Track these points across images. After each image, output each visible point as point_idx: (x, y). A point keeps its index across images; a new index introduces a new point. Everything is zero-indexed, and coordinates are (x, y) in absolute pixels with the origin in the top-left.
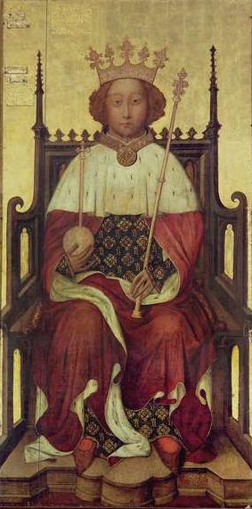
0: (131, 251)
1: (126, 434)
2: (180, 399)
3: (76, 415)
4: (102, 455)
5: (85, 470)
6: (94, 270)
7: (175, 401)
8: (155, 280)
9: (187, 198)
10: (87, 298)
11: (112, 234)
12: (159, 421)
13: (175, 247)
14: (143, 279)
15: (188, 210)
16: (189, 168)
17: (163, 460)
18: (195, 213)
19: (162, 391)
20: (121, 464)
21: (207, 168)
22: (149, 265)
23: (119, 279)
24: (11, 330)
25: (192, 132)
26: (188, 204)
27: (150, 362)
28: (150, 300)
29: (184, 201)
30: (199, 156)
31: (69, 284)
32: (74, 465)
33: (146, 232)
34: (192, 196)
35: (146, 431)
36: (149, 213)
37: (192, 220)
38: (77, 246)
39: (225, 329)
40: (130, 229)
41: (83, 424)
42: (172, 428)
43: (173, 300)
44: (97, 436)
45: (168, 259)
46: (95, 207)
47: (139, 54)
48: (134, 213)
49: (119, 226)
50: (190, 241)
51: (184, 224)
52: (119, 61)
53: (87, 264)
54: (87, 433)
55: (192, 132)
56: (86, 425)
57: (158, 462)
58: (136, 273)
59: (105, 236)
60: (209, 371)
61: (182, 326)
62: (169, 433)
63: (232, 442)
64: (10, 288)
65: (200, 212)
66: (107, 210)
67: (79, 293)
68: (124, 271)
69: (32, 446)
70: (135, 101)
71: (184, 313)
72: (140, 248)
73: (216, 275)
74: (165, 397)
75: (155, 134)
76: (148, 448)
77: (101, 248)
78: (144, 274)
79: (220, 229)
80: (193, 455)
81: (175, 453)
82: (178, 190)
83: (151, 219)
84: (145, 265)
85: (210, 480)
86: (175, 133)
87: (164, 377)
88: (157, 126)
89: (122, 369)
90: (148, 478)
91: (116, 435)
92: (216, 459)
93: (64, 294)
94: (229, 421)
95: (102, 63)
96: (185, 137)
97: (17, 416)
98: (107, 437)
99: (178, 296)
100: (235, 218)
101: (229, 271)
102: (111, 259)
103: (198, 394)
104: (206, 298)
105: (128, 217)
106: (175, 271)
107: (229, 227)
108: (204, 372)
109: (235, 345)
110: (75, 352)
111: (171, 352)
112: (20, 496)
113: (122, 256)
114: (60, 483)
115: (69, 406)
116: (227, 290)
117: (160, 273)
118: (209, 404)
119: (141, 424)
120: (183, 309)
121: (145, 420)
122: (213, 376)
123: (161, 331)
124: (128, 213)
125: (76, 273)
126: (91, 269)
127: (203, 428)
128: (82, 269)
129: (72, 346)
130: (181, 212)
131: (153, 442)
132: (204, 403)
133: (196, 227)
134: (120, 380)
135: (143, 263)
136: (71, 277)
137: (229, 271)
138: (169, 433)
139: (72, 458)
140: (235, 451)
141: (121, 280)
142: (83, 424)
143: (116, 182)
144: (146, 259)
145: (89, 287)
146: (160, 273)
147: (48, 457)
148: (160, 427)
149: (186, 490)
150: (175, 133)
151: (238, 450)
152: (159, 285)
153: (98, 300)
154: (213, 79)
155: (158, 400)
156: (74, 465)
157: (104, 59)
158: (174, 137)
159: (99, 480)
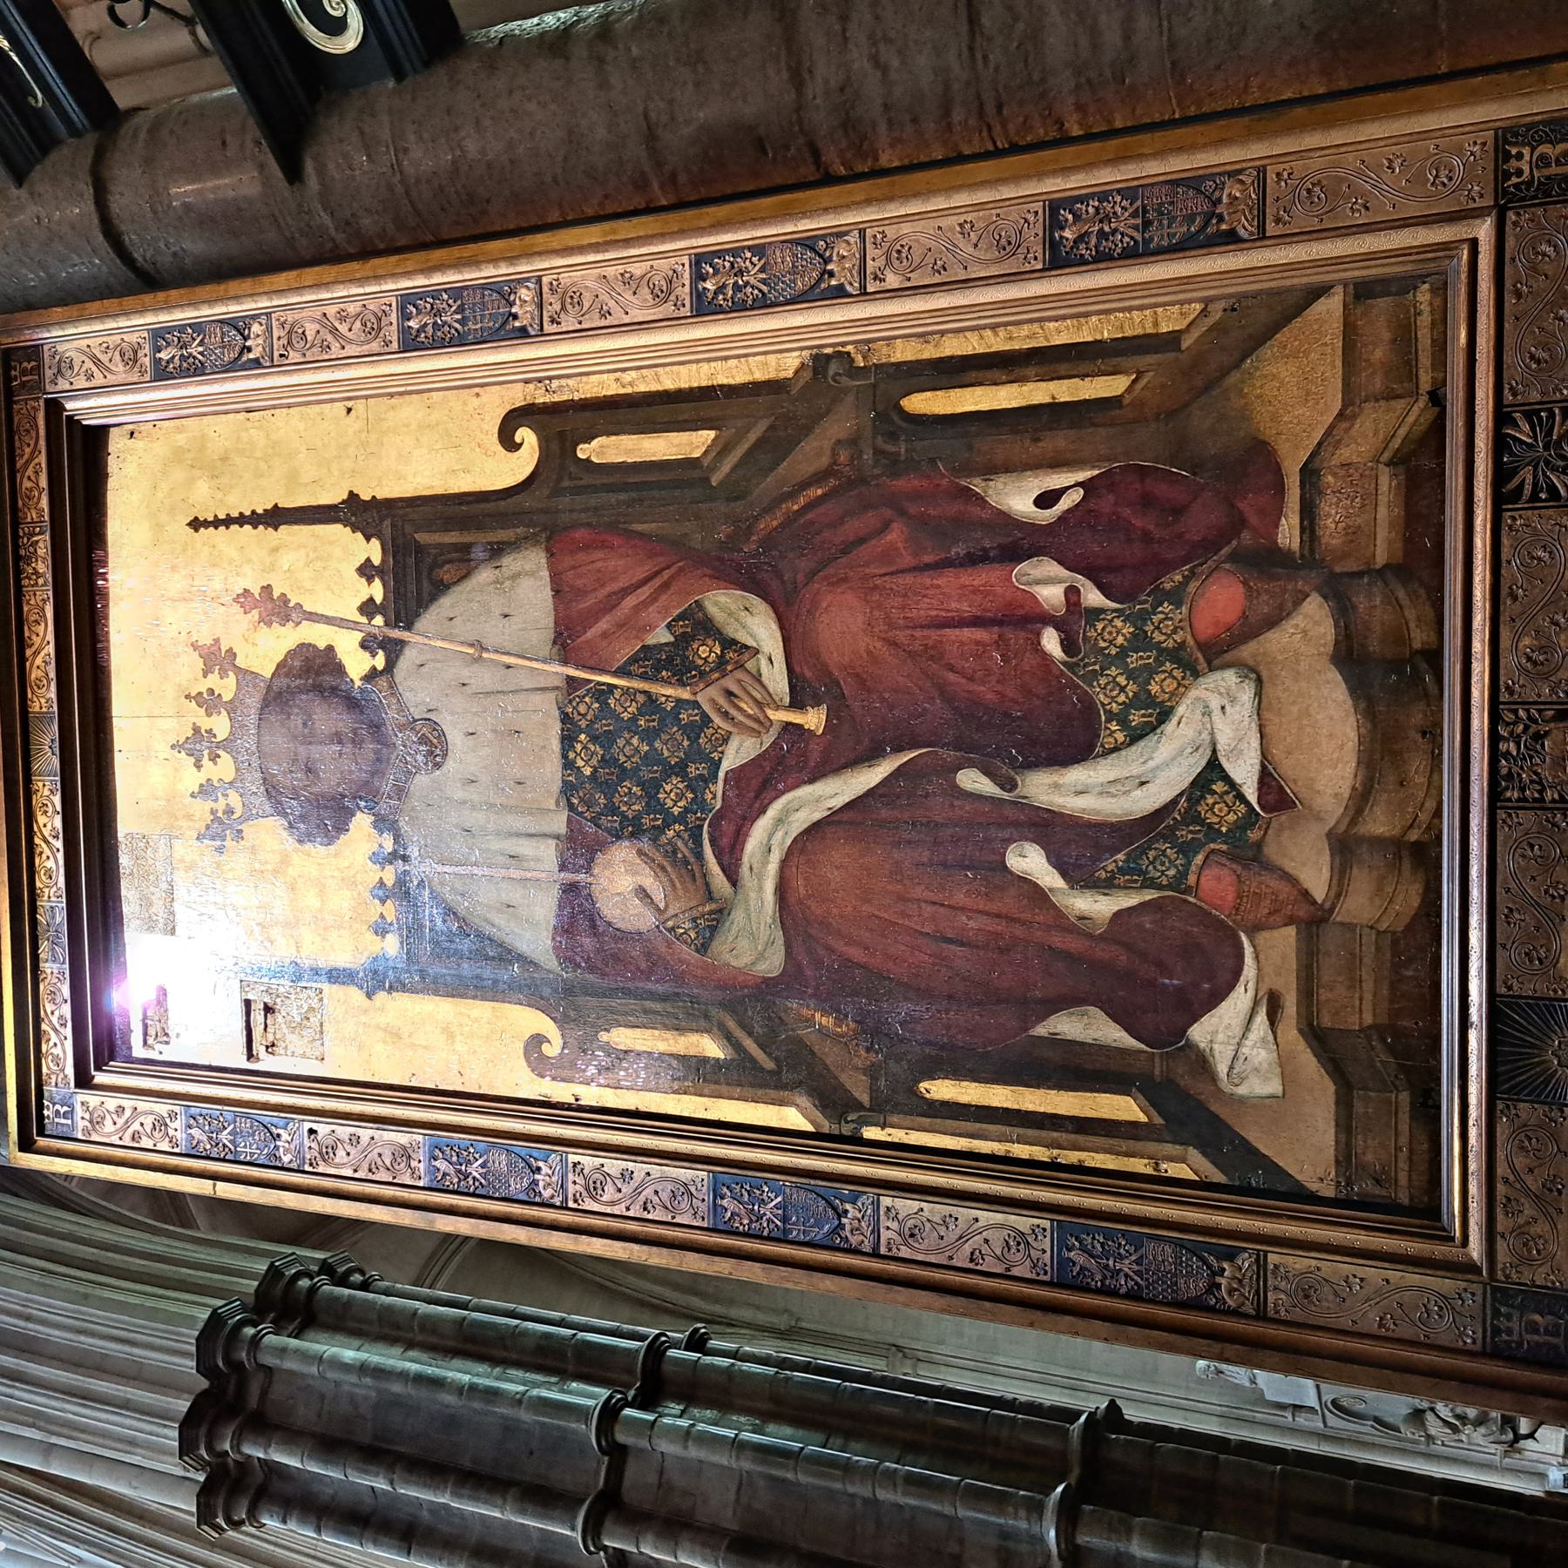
0: (649, 736)
1: (1181, 752)
2: (1064, 573)
3: (1118, 915)
4: (1253, 835)
5: (1306, 894)
6: (701, 845)
7: (1072, 592)
8: (721, 661)
9: (515, 577)
10: (773, 867)
11: (609, 788)
12: (1140, 641)
13: (637, 609)
14: (722, 701)
15: (545, 574)
16: (447, 572)
17: (1273, 621)
18: (551, 554)
19: (1038, 634)
20: (1289, 768)
21: (448, 524)
22: (682, 684)
23: (721, 775)
24: (865, 1098)
25: (367, 571)
26: (532, 574)
27: (951, 677)
28: (777, 679)
29: (526, 584)
30: (420, 549)
31: (738, 917)
32: (1291, 931)
33: (606, 691)
34: (511, 562)
35: (1170, 685)
36: (557, 683)
37: (568, 561)
38: (642, 893)
39: (853, 442)
40: (594, 739)
41: (1149, 895)
42: (1161, 596)
43: (776, 611)
44: (1187, 850)
45: (669, 626)
46: (545, 835)
47: (209, 714)
48: (556, 728)
49: (588, 771)
50: (622, 566)
51: (579, 583)
52: (225, 768)
53: (686, 862)
54: (1178, 883)
55: (367, 571)
56: (1150, 884)
57: (1278, 641)
58: (706, 720)
59: (614, 810)
60: (977, 485)
61: (845, 580)
62: (1178, 605)
63: (1207, 388)
64: (749, 1092)
65: (549, 539)
66: (551, 804)
67: (761, 888)
68: (695, 754)
69: (1222, 1069)
70: (305, 724)
71: (813, 574)
72: (641, 712)
73: (708, 480)
74: (1059, 624)
75: (374, 668)
76: (1230, 677)
77: (646, 821)
78: (708, 697)
79: (588, 480)
80: (1253, 520)
81: (1245, 583)
82: (497, 605)
83: (570, 680)
84: (685, 694)
85: (1345, 453)
86: (371, 617)
87: (996, 629)
88: (357, 664)
89: (971, 764)
90: (1334, 675)
91: (1186, 784)
92: (1268, 431)
93: (764, 934)
94: (1139, 404)
95: (229, 811)
96: (377, 591)
97: (1124, 1107)
98: (1192, 817)
99: (765, 596)
100: (562, 434)
101: (693, 443)
102: (672, 794)
103: (1048, 516)
104: (768, 510)
105: (568, 740)
106: (699, 605)
107: (583, 451)
108: (981, 501)
109: (901, 411)
110: (928, 910)
111: (924, 609)
112: (1404, 1127)
113: (664, 762)
114: (1355, 983)
115: (1090, 936)
116: (746, 446)
117: (706, 652)
118: (1083, 476)
119: (1144, 700)
120: (800, 577)
121: (1132, 688)
122: (991, 470)
123: (863, 643)
124: (556, 745)
125: (710, 896)
126: (699, 856)
127: (1162, 490)
128: (699, 881)
129: (904, 914)
130: (548, 593)
131: (1209, 663)
132: (1076, 496)
133: (587, 547)
134: (1005, 770)
135: (679, 701)
136: (720, 911)
137: (693, 443)
138: (1178, 605)
139: (1263, 937)
140: (1234, 377)
141: (726, 765)
142: (1149, 895)
143: (484, 779)
144: (669, 691)
145: (745, 859)
146: (706, 652)
147: (1261, 1018)
148: (1158, 637)
149: (1382, 534)
150: (371, 617)
151: (1237, 365)
152: (736, 652)
153: (779, 834)
154: (254, 520)
155: (1068, 645)
156: (1291, 931)
157: (221, 805)
158: (379, 620)
159: (1344, 847)
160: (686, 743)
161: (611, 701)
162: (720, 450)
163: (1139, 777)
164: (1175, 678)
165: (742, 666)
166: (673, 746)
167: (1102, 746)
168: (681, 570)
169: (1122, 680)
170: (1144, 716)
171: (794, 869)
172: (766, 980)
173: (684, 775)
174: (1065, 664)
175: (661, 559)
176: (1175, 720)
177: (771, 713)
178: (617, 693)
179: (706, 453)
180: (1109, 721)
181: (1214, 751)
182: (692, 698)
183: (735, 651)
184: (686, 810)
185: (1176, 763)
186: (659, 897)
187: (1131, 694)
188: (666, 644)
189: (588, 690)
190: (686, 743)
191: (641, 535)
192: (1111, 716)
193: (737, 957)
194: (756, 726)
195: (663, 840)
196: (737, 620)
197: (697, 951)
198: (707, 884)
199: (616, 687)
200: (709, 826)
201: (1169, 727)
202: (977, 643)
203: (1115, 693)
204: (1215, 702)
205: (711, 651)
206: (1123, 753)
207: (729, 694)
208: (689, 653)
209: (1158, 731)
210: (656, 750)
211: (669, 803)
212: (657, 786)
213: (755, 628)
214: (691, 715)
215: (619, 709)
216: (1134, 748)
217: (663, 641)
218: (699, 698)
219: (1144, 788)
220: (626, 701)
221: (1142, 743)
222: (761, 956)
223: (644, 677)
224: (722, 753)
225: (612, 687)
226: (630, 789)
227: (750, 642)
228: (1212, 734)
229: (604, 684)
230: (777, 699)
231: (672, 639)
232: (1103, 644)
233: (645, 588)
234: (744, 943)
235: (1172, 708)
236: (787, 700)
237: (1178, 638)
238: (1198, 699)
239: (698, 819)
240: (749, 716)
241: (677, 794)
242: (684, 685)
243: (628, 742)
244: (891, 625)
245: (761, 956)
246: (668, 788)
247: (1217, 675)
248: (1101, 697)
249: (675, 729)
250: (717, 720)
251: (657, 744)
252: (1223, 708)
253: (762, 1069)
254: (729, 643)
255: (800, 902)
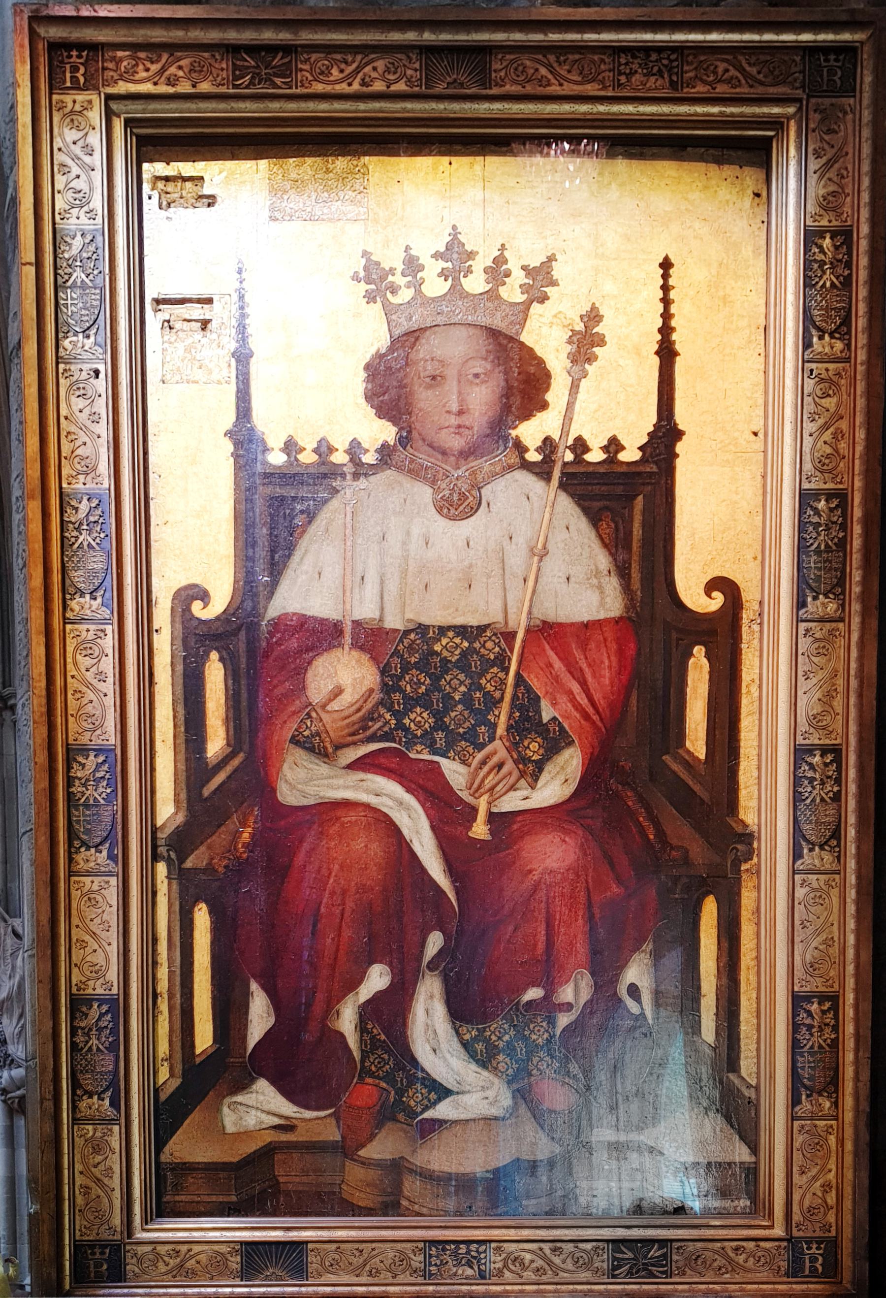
0: (467, 700)
6: (379, 741)
10: (364, 797)
11: (423, 665)
13: (570, 693)
14: (495, 760)
22: (509, 728)
28: (511, 803)
31: (323, 769)
38: (338, 692)
40: (464, 654)
53: (365, 728)
58: (480, 747)
59: (406, 668)
67: (347, 787)
72: (487, 694)
78: (498, 749)
84: (501, 730)
93: (310, 790)
106: (570, 743)
113: (447, 710)
117: (534, 748)
125: (338, 747)
126: (372, 739)
128: (350, 739)
135: (494, 726)
141: (444, 763)
144: (503, 718)
145: (370, 776)
146: (534, 748)
153: (390, 803)
160: (461, 730)
161: (495, 670)
162: (689, 763)
163: (439, 1049)
164: (507, 1070)
165: (522, 776)
166: (459, 720)
167: (461, 1026)
168: (599, 729)
169: (506, 1038)
170: (481, 1051)
171: (363, 814)
172: (274, 790)
173: (434, 729)
174: (518, 1002)
175: (608, 713)
176: (479, 1070)
177: (485, 797)
178: (501, 675)
179: (688, 752)
180: (478, 1029)
181: (458, 1093)
182: (498, 736)
183: (534, 771)
184: (407, 730)
185: (449, 1070)
186: (335, 706)
187: (497, 1043)
188: (540, 716)
189: (504, 650)
190: (461, 730)
191: (628, 697)
192: (481, 1031)
193: (290, 768)
194: (475, 786)
195: (382, 711)
196: (558, 773)
197: (293, 737)
198: (348, 745)
199: (507, 674)
200: (395, 748)
201: (473, 1066)
202: (535, 945)
203: (497, 1033)
204: (490, 1093)
205: (534, 752)
206: (456, 1039)
207: (500, 766)
208: (533, 735)
209: (471, 1060)
210: (456, 706)
211: (413, 716)
212: (427, 706)
213: (551, 787)
214: (484, 735)
215: (489, 677)
216: (459, 1045)
217: (544, 714)
218: (497, 743)
219: (432, 1052)
220: (496, 682)
221: (462, 1050)
222: (292, 787)
223: (515, 697)
224: (454, 759)
225: (506, 670)
226: (423, 684)
227: (540, 783)
228: (469, 1092)
229: (509, 664)
230: (496, 803)
231: (545, 721)
232: (531, 1026)
233: (586, 701)
234: (301, 774)
235: (487, 1068)
236: (495, 810)
237: (534, 1072)
238: (493, 1084)
239: (400, 739)
240: (483, 781)
241: (420, 722)
242: (508, 730)
243: (462, 683)
244: (549, 886)
245: (292, 787)
246: (425, 715)
247: (509, 1095)
248: (495, 1026)
249: (473, 722)
250: (480, 756)
251: (460, 707)
252: (487, 1098)
253: (203, 786)
254: (540, 767)
255: (338, 819)
